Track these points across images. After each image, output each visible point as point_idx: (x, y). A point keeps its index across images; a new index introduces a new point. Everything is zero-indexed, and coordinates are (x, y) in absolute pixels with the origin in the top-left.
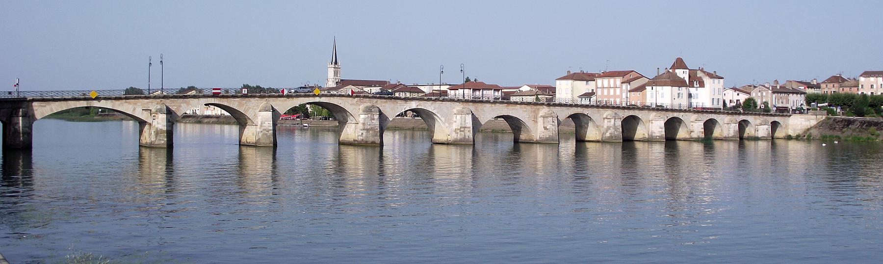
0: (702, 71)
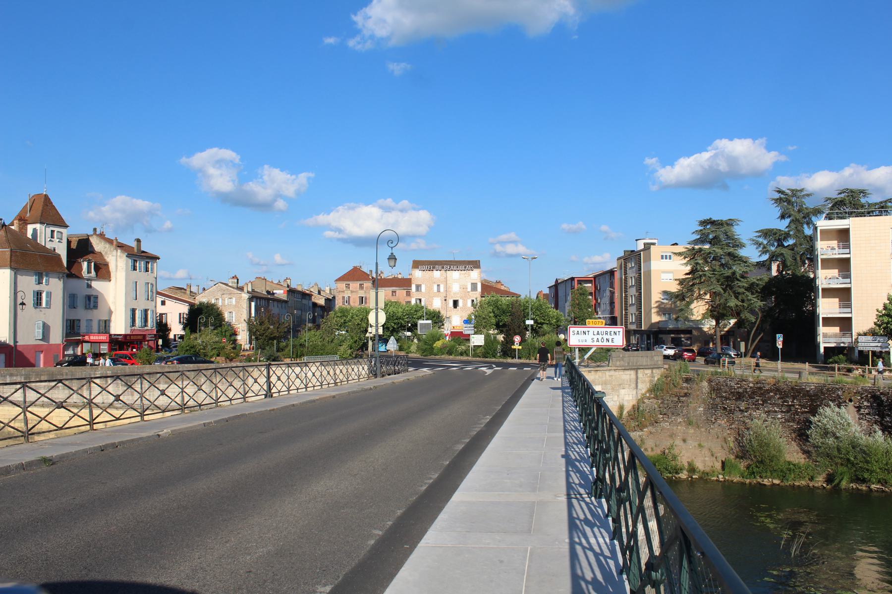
0: (102, 236)
